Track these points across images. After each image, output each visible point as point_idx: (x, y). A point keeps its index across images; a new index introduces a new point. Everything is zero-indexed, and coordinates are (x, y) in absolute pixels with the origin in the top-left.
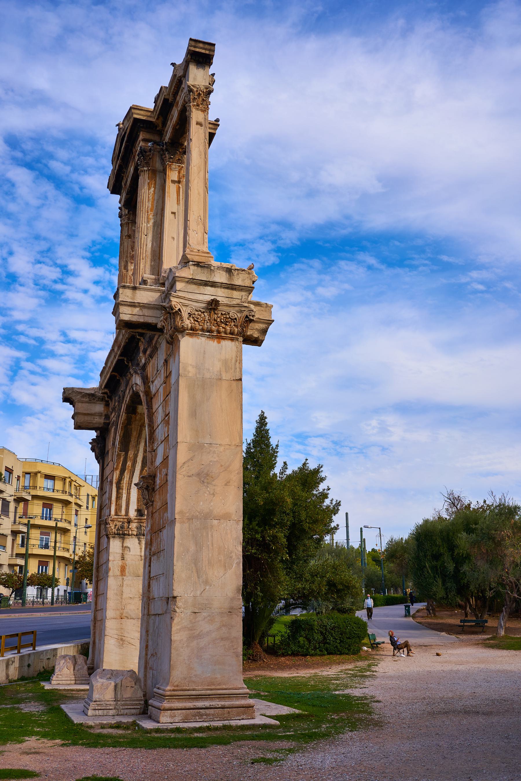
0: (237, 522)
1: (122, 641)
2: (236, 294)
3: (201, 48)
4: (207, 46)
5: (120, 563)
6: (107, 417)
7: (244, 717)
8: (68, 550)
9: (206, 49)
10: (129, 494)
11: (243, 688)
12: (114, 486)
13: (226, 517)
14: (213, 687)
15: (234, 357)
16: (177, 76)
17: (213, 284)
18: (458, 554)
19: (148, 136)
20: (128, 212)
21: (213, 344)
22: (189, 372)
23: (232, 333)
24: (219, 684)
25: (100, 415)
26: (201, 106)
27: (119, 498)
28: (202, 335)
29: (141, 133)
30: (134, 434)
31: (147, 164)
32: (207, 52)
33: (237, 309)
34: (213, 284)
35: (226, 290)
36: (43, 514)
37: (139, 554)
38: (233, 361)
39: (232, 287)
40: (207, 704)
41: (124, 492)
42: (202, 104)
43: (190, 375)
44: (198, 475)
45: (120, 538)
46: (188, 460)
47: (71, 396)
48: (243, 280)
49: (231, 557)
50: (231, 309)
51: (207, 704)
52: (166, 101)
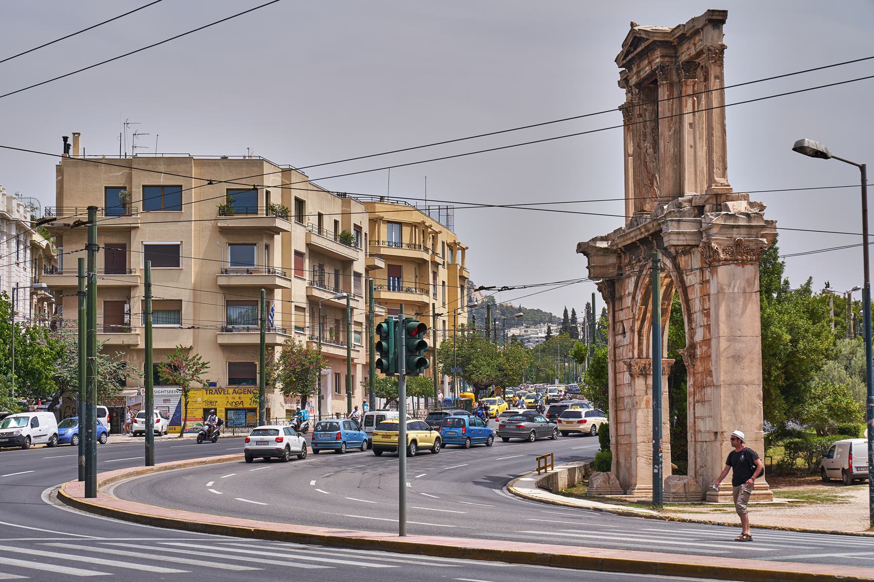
0: (759, 385)
4: (721, 14)
6: (620, 268)
12: (636, 333)
13: (752, 383)
17: (738, 227)
19: (665, 51)
20: (639, 92)
21: (740, 269)
25: (613, 265)
29: (659, 50)
38: (753, 279)
44: (733, 357)
46: (727, 348)
47: (586, 250)
52: (683, 35)
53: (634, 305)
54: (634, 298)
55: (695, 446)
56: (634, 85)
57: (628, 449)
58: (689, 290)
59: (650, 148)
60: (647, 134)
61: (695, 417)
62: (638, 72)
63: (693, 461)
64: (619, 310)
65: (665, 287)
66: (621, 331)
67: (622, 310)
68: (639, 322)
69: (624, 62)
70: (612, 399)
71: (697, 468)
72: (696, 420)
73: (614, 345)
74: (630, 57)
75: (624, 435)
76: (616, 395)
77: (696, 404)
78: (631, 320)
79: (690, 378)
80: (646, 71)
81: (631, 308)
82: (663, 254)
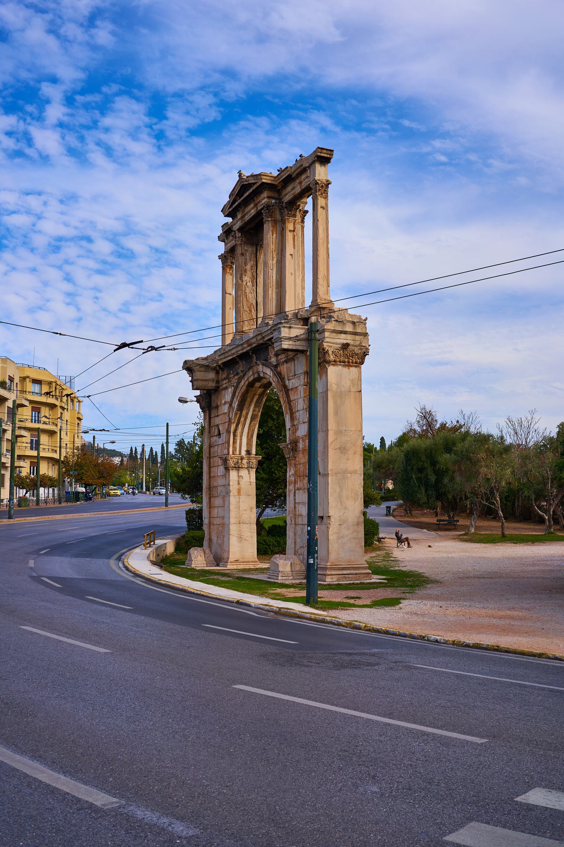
1: (240, 538)
2: (358, 338)
3: (325, 153)
4: (328, 152)
5: (237, 487)
6: (218, 382)
7: (367, 579)
8: (56, 451)
9: (328, 154)
10: (241, 439)
11: (365, 564)
12: (232, 434)
13: (355, 472)
14: (350, 564)
15: (357, 377)
16: (303, 166)
17: (345, 333)
18: (439, 468)
19: (271, 194)
20: (241, 235)
21: (345, 370)
22: (333, 388)
23: (356, 363)
24: (353, 562)
25: (213, 380)
26: (323, 195)
27: (234, 442)
28: (340, 365)
29: (266, 191)
30: (249, 399)
31: (271, 216)
32: (328, 156)
33: (359, 347)
34: (345, 333)
35: (352, 336)
36: (32, 416)
37: (249, 480)
38: (357, 380)
39: (355, 334)
40: (348, 572)
41: (238, 438)
42: (324, 193)
43: (334, 389)
44: (340, 448)
45: (236, 470)
46: (334, 440)
48: (362, 329)
49: (358, 494)
50: (356, 347)
51: (348, 572)
52: (289, 176)
53: (231, 411)
54: (231, 405)
55: (295, 528)
56: (238, 230)
57: (220, 529)
58: (291, 394)
59: (249, 282)
60: (247, 270)
61: (295, 503)
62: (243, 217)
63: (293, 542)
64: (214, 417)
65: (257, 396)
66: (216, 433)
67: (218, 416)
68: (235, 425)
69: (230, 210)
70: (206, 488)
71: (297, 548)
72: (297, 505)
73: (210, 445)
74: (237, 203)
75: (218, 517)
76: (210, 485)
77: (297, 492)
78: (227, 424)
79: (290, 469)
80: (251, 214)
81: (227, 414)
82: (263, 365)
